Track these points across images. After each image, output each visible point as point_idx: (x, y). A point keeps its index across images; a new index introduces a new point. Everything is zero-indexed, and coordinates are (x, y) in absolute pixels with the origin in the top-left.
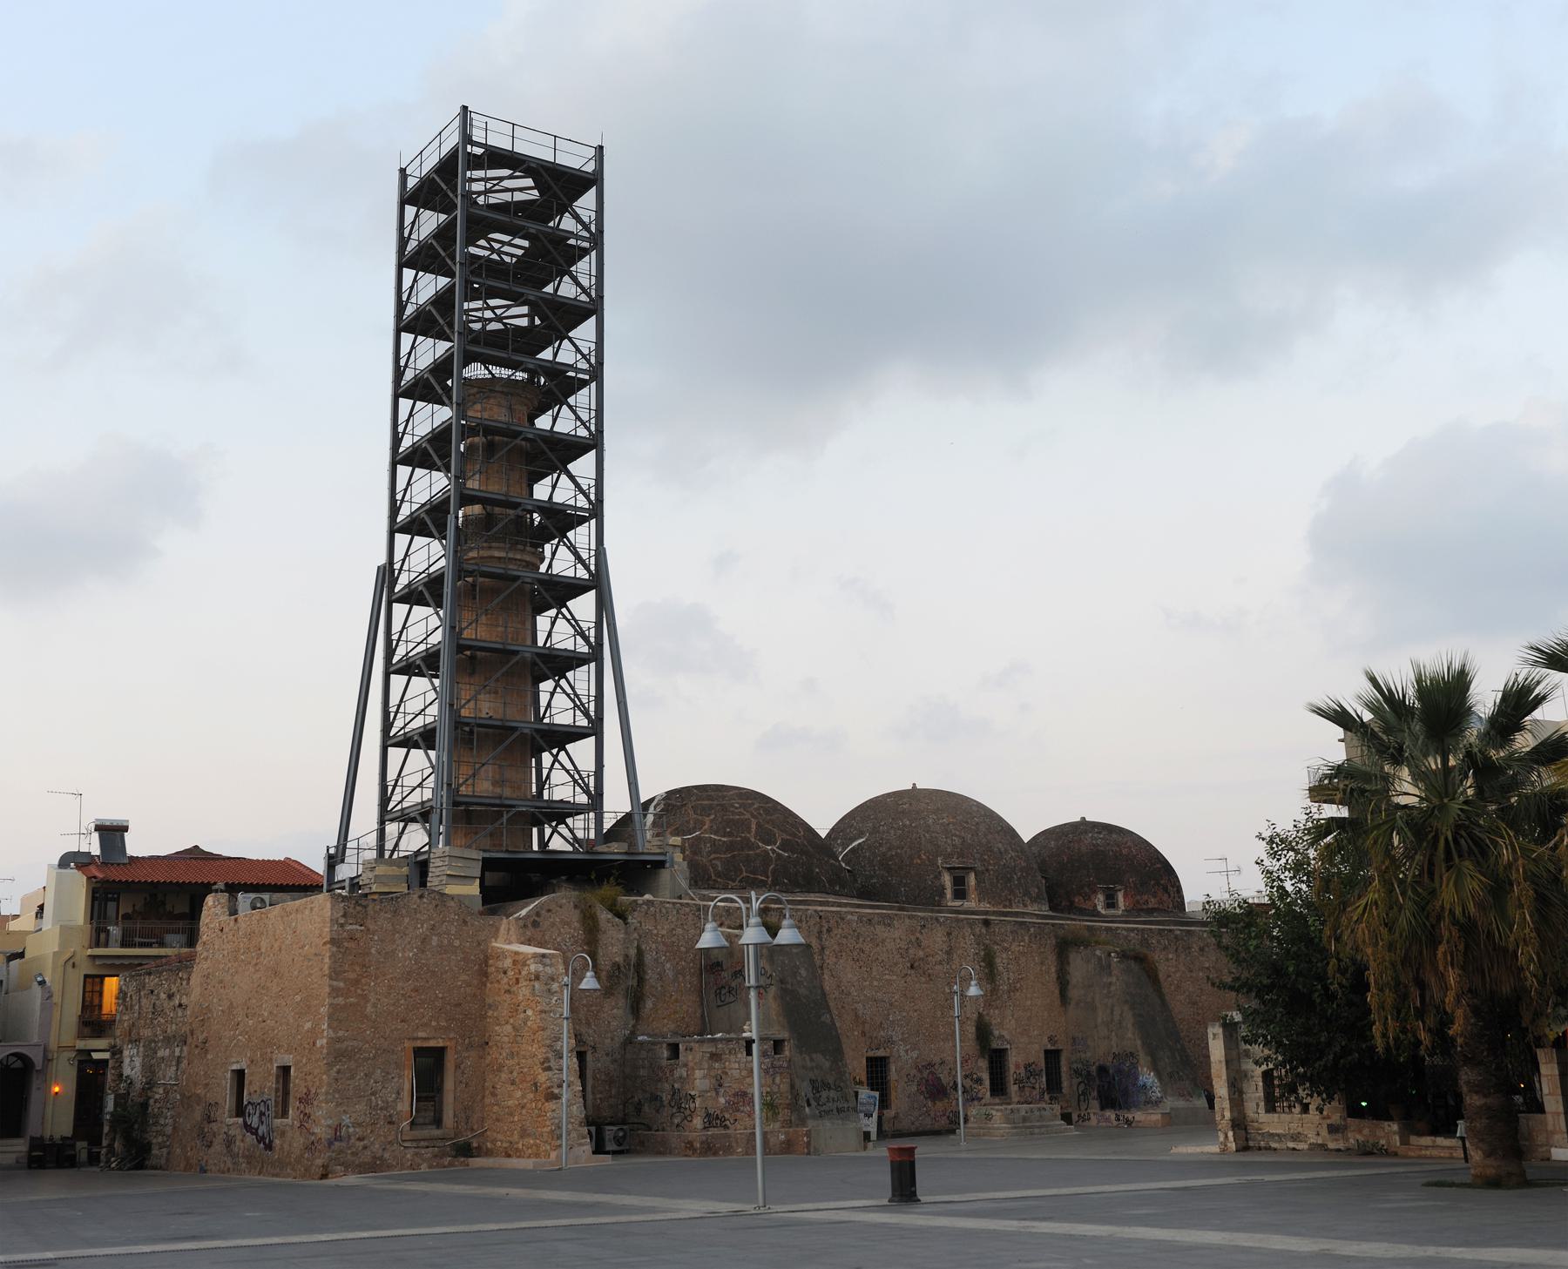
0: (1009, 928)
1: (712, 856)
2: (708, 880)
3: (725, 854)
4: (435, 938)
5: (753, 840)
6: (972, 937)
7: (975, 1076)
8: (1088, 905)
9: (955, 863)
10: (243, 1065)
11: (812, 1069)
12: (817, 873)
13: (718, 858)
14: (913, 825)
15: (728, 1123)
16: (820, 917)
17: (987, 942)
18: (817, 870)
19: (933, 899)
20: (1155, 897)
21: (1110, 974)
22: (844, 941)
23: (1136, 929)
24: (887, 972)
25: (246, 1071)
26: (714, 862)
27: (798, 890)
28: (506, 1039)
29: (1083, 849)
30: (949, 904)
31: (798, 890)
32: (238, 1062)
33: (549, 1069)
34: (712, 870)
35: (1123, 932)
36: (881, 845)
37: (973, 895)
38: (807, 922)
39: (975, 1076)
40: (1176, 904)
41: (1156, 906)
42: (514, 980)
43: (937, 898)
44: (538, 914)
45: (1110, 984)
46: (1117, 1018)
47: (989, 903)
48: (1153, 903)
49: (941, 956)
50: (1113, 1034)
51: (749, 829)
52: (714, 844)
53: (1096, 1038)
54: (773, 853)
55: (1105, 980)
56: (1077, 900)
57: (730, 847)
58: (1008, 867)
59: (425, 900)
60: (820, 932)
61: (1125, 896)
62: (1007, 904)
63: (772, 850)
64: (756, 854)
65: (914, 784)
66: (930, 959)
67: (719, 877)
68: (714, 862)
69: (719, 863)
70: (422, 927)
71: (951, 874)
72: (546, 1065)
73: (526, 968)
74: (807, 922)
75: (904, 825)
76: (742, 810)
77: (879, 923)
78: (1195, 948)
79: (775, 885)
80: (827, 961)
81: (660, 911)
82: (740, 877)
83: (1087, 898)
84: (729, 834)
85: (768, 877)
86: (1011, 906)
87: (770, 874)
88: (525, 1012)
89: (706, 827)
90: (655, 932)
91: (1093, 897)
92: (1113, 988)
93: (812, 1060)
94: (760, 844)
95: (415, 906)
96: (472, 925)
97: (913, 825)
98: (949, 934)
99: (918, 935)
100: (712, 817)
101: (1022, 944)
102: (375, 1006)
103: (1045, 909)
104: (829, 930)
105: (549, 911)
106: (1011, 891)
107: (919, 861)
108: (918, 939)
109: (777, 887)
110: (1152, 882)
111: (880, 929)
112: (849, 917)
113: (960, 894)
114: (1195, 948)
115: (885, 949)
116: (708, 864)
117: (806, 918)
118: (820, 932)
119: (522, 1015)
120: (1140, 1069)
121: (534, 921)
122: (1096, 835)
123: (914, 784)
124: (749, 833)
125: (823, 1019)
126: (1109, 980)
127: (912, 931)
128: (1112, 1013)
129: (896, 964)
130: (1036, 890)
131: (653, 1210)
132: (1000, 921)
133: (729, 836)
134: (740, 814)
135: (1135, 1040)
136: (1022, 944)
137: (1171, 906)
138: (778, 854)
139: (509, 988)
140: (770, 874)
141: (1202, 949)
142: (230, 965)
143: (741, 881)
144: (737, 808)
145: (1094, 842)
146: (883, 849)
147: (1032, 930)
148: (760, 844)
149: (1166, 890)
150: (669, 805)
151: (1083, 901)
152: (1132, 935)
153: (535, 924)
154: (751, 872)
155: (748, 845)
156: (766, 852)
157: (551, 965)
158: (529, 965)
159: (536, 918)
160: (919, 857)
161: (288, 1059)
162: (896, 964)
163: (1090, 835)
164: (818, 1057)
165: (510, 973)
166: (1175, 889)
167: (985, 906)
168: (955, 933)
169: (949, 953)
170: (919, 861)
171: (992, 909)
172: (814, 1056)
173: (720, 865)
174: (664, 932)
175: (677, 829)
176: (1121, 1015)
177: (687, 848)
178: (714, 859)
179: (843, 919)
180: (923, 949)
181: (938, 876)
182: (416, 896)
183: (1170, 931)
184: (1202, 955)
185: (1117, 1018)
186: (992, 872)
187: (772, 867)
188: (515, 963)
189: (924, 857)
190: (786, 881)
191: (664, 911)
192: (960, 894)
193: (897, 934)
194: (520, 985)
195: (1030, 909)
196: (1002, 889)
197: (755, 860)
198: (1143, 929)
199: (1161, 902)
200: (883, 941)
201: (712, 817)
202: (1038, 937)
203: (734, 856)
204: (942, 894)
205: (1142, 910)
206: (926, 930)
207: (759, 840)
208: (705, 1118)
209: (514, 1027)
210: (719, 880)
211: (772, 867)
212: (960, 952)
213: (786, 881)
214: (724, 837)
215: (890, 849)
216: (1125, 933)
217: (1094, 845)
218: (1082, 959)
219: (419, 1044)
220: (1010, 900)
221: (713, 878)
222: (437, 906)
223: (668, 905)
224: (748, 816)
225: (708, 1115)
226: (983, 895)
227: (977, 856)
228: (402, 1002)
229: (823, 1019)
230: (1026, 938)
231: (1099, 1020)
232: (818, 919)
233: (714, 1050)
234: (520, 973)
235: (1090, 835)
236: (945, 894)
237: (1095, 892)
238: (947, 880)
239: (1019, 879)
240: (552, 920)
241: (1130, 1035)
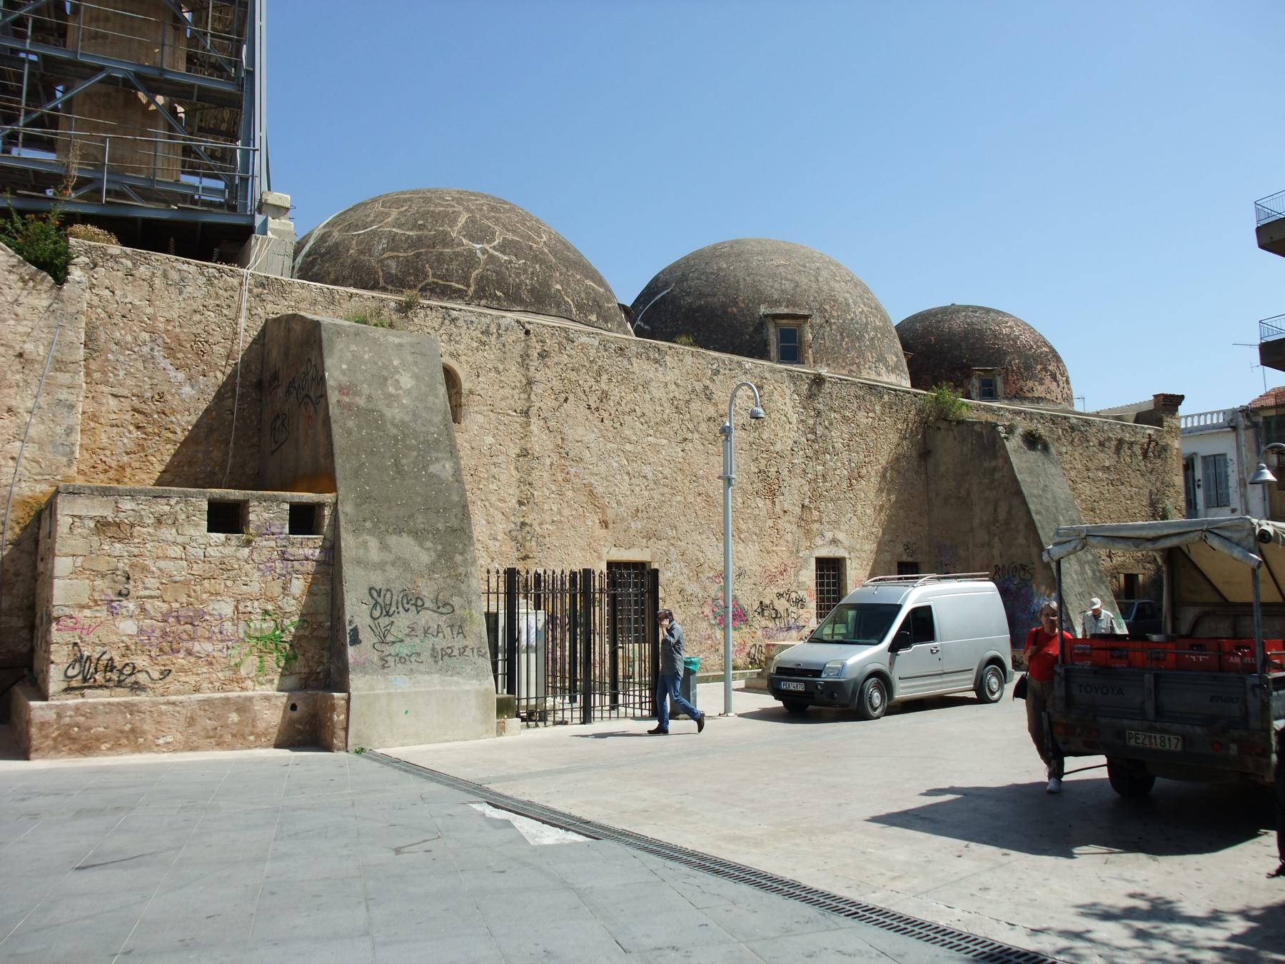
0: (852, 390)
6: (795, 396)
7: (793, 595)
11: (381, 566)
12: (558, 290)
14: (731, 268)
15: (142, 678)
16: (527, 333)
18: (558, 287)
21: (994, 456)
22: (573, 376)
24: (651, 432)
27: (518, 308)
31: (518, 308)
34: (381, 274)
35: (1007, 414)
38: (500, 336)
39: (793, 595)
40: (1065, 395)
41: (1043, 395)
45: (995, 469)
46: (1002, 515)
50: (996, 538)
51: (453, 221)
52: (393, 240)
53: (971, 545)
54: (483, 254)
55: (986, 464)
58: (857, 323)
60: (525, 356)
63: (484, 251)
64: (454, 253)
69: (393, 264)
71: (776, 325)
74: (500, 336)
76: (454, 203)
77: (639, 355)
78: (1094, 442)
79: (480, 298)
80: (537, 404)
81: (165, 275)
82: (423, 284)
84: (421, 227)
91: (966, 382)
92: (997, 475)
93: (384, 547)
94: (464, 241)
101: (870, 415)
104: (543, 355)
106: (861, 354)
108: (706, 388)
109: (483, 302)
110: (1039, 367)
112: (584, 339)
114: (1094, 442)
115: (648, 397)
117: (499, 328)
118: (525, 356)
120: (1034, 587)
122: (970, 314)
125: (433, 469)
126: (994, 464)
127: (697, 375)
128: (995, 510)
130: (895, 359)
132: (840, 379)
135: (1029, 546)
136: (870, 415)
137: (1059, 397)
138: (491, 257)
144: (447, 200)
145: (969, 321)
147: (886, 397)
148: (464, 241)
149: (1054, 378)
154: (439, 277)
155: (445, 240)
156: (472, 253)
162: (667, 422)
163: (964, 314)
164: (404, 544)
166: (1064, 379)
172: (393, 540)
176: (1009, 512)
178: (388, 258)
180: (716, 405)
183: (1065, 418)
184: (1102, 452)
185: (1002, 515)
186: (834, 327)
187: (477, 272)
189: (743, 305)
190: (499, 294)
193: (670, 377)
195: (885, 379)
196: (847, 349)
200: (646, 385)
202: (895, 408)
203: (418, 255)
206: (721, 377)
207: (464, 236)
208: (72, 665)
211: (477, 272)
213: (499, 294)
214: (411, 230)
217: (968, 324)
218: (955, 439)
224: (459, 208)
225: (80, 659)
229: (433, 469)
230: (878, 408)
231: (976, 521)
232: (522, 336)
233: (109, 514)
235: (964, 314)
241: (1021, 540)
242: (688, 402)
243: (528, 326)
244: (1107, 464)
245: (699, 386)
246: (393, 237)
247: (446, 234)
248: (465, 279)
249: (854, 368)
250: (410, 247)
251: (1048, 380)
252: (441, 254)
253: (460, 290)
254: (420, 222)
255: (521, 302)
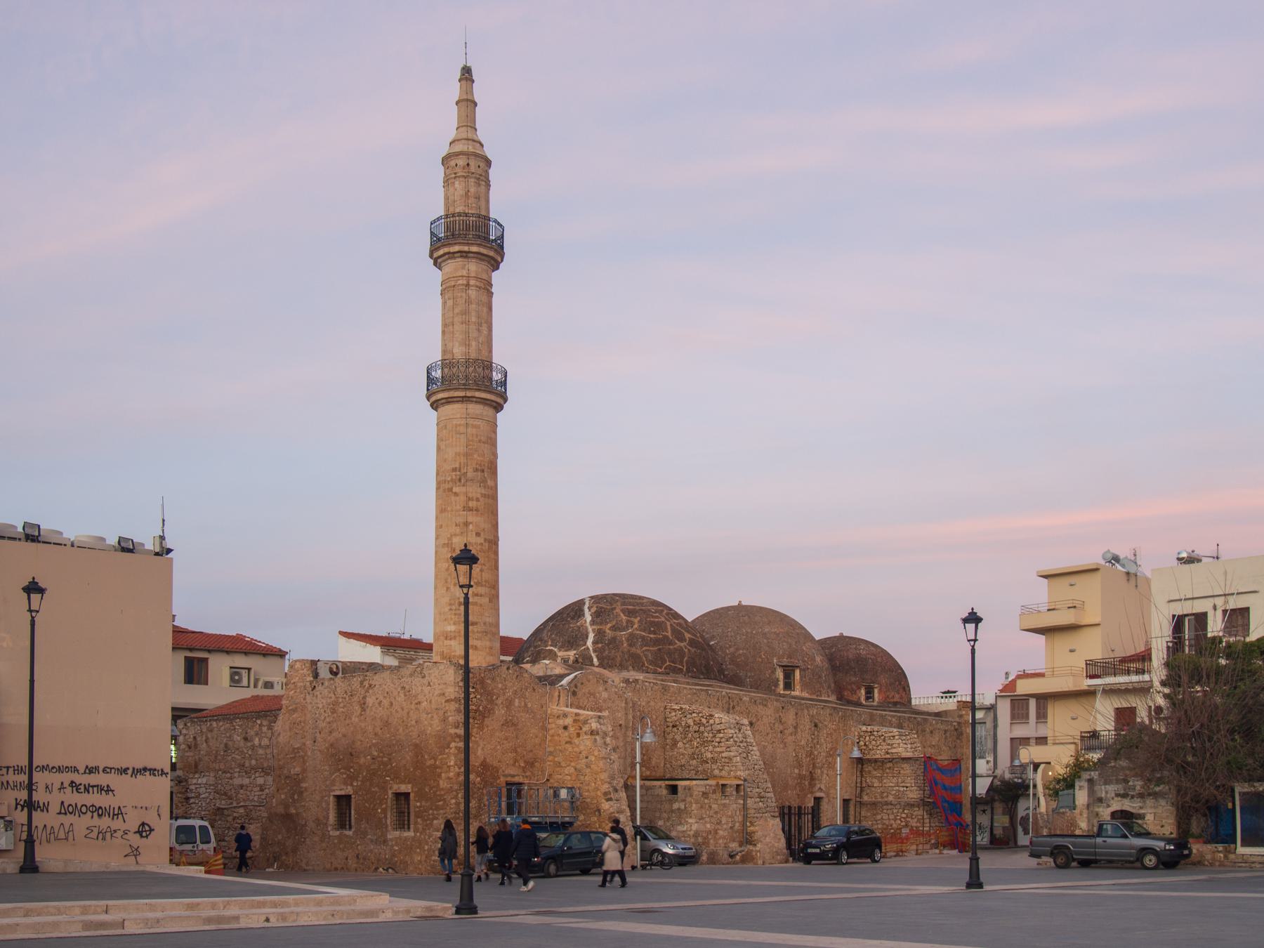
1: (644, 648)
2: (642, 666)
3: (653, 647)
4: (517, 700)
5: (671, 638)
8: (854, 698)
9: (785, 661)
10: (349, 790)
13: (648, 650)
17: (817, 721)
19: (770, 687)
20: (899, 693)
23: (896, 715)
25: (353, 796)
26: (646, 653)
27: (702, 677)
28: (569, 778)
29: (851, 656)
30: (782, 692)
32: (341, 790)
33: (610, 799)
34: (645, 659)
36: (730, 647)
37: (798, 687)
42: (575, 734)
43: (773, 688)
44: (576, 686)
47: (807, 692)
48: (897, 698)
49: (791, 730)
56: (846, 694)
57: (656, 642)
59: (510, 671)
61: (880, 692)
62: (819, 693)
65: (740, 602)
66: (786, 731)
67: (650, 664)
68: (646, 653)
70: (509, 691)
72: (609, 796)
73: (587, 726)
75: (747, 632)
77: (760, 703)
83: (854, 692)
85: (683, 666)
86: (821, 696)
87: (685, 664)
88: (587, 758)
89: (636, 626)
90: (639, 703)
91: (858, 691)
94: (677, 641)
95: (505, 676)
96: (538, 692)
97: (754, 632)
98: (797, 714)
99: (781, 714)
100: (639, 618)
102: (483, 749)
103: (833, 698)
104: (733, 708)
105: (582, 684)
107: (760, 660)
108: (780, 716)
109: (690, 674)
111: (761, 707)
112: (745, 698)
113: (788, 686)
116: (642, 654)
118: (729, 709)
119: (584, 760)
121: (574, 691)
123: (740, 602)
124: (667, 632)
129: (768, 734)
131: (909, 890)
133: (655, 634)
134: (657, 617)
138: (689, 649)
139: (569, 740)
140: (685, 664)
141: (931, 732)
142: (326, 715)
143: (665, 668)
146: (732, 650)
147: (840, 713)
150: (601, 608)
151: (850, 694)
152: (894, 720)
153: (574, 693)
154: (673, 662)
157: (604, 724)
158: (591, 724)
159: (575, 689)
160: (760, 657)
161: (404, 788)
165: (571, 729)
167: (805, 695)
168: (799, 714)
169: (796, 728)
170: (760, 660)
171: (809, 697)
173: (650, 655)
174: (644, 704)
175: (614, 626)
177: (625, 642)
179: (741, 700)
181: (774, 671)
182: (505, 667)
183: (915, 718)
188: (575, 721)
190: (695, 670)
191: (644, 688)
192: (788, 686)
194: (581, 738)
197: (674, 653)
198: (900, 717)
199: (901, 698)
201: (639, 618)
203: (659, 650)
204: (776, 685)
205: (889, 703)
209: (576, 769)
210: (650, 667)
212: (802, 727)
213: (695, 670)
215: (737, 649)
216: (890, 718)
219: (509, 779)
220: (820, 691)
221: (646, 665)
222: (517, 676)
223: (646, 684)
224: (663, 619)
226: (805, 686)
227: (800, 658)
228: (498, 747)
230: (837, 719)
234: (581, 729)
236: (779, 685)
237: (859, 688)
238: (780, 674)
239: (825, 676)
240: (584, 691)
242: (774, 724)
243: (730, 695)
244: (933, 744)
245: (777, 715)
246: (643, 638)
247: (667, 637)
248: (681, 663)
249: (819, 693)
250: (654, 644)
251: (901, 690)
252: (669, 648)
253: (680, 669)
254: (652, 629)
255: (702, 673)
